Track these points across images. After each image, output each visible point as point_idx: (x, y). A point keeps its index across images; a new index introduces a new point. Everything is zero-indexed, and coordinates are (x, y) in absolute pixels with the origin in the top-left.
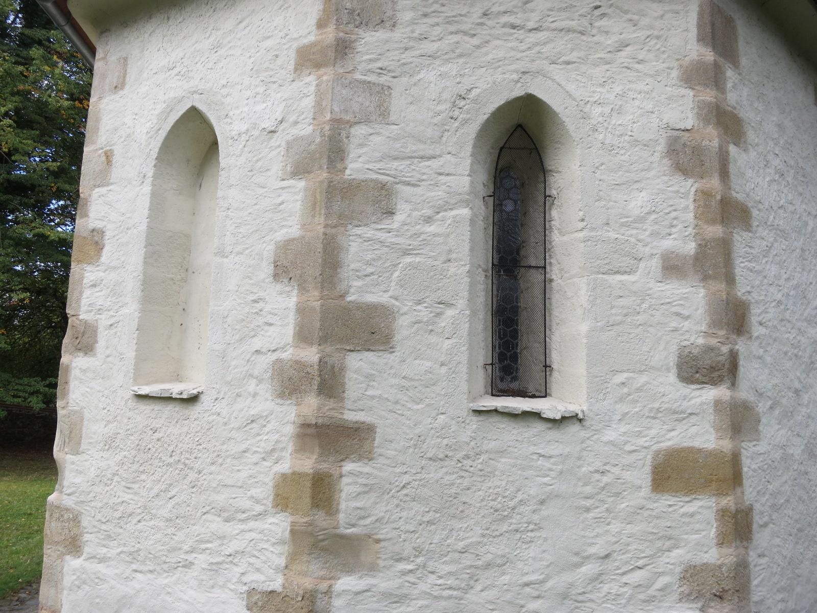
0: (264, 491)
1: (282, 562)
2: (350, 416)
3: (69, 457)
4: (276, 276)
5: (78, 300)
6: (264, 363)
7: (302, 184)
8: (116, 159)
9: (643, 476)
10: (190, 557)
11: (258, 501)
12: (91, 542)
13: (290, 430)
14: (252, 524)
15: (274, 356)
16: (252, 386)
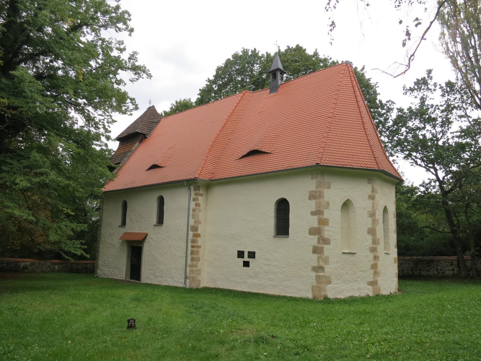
0: (369, 267)
1: (372, 277)
2: (378, 255)
3: (326, 266)
4: (368, 233)
5: (324, 233)
6: (368, 247)
7: (371, 219)
8: (330, 204)
10: (356, 279)
11: (368, 268)
12: (334, 281)
13: (372, 257)
14: (368, 272)
15: (369, 246)
16: (366, 251)
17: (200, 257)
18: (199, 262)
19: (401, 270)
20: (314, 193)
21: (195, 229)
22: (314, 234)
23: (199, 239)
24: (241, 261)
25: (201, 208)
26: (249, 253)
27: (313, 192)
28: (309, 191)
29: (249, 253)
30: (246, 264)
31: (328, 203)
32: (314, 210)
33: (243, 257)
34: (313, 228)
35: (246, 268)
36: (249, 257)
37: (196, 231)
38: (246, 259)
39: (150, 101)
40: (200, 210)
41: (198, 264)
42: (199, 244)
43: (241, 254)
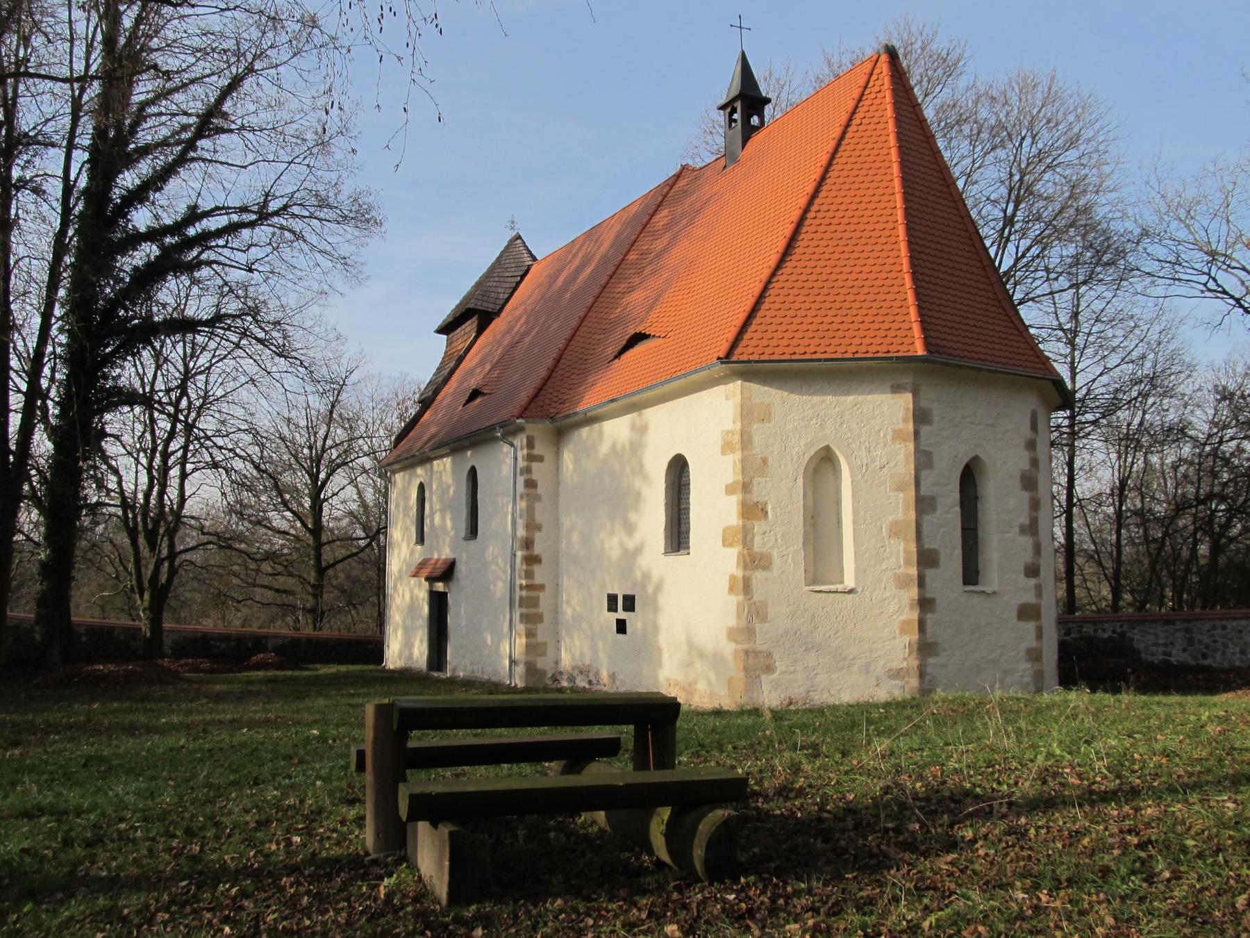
9: (1014, 614)
17: (542, 614)
18: (540, 626)
19: (1238, 649)
20: (730, 435)
21: (528, 544)
22: (731, 545)
23: (537, 569)
24: (614, 617)
25: (541, 490)
26: (626, 598)
27: (728, 432)
28: (722, 432)
29: (626, 598)
30: (621, 627)
31: (765, 461)
32: (731, 481)
33: (616, 610)
34: (729, 528)
35: (621, 636)
36: (626, 609)
37: (528, 548)
38: (621, 614)
39: (513, 222)
40: (538, 498)
41: (536, 629)
42: (538, 580)
43: (612, 600)
